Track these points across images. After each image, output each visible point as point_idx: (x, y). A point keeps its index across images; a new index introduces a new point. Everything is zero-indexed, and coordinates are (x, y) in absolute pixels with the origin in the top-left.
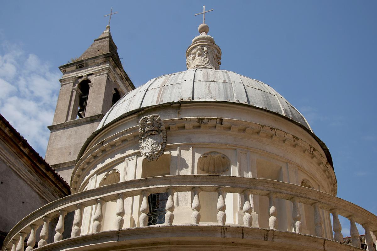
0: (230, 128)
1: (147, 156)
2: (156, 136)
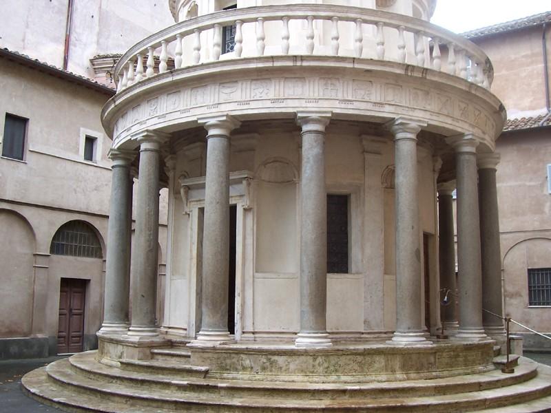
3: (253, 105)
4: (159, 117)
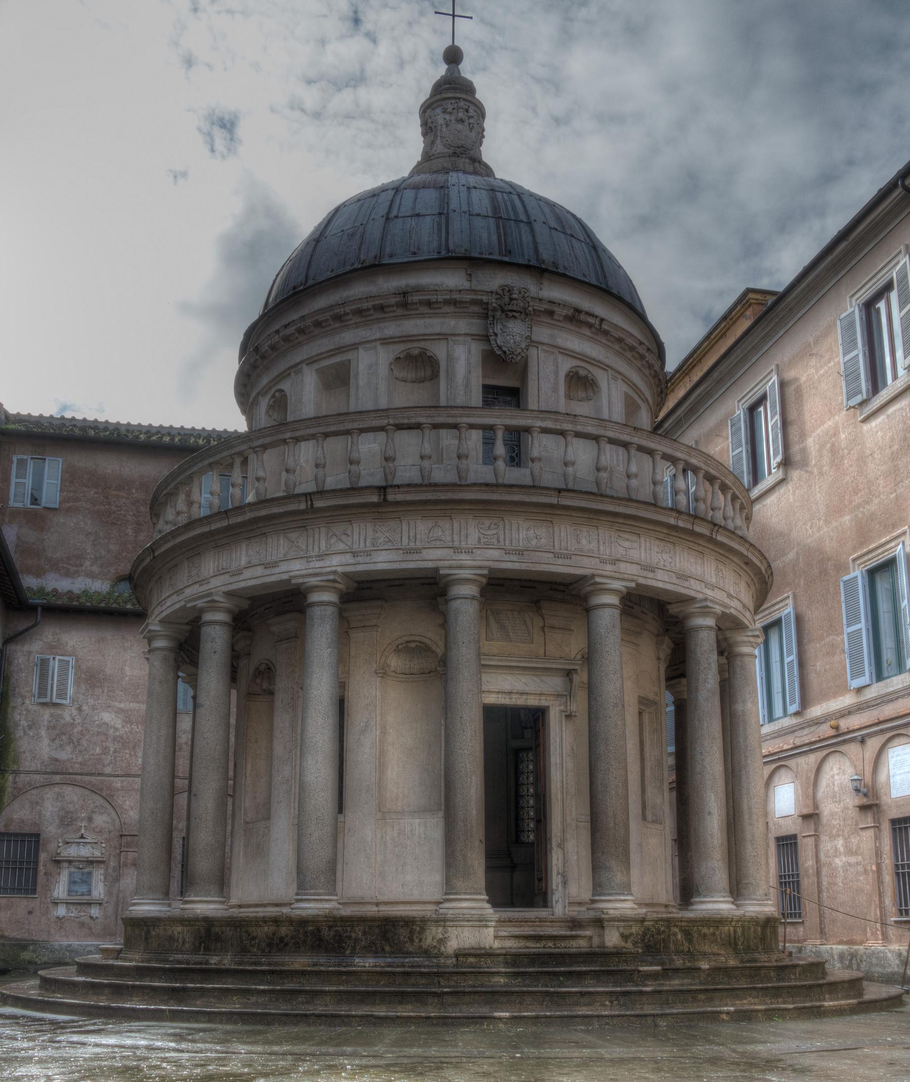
1: (505, 352)
3: (660, 575)
4: (507, 552)
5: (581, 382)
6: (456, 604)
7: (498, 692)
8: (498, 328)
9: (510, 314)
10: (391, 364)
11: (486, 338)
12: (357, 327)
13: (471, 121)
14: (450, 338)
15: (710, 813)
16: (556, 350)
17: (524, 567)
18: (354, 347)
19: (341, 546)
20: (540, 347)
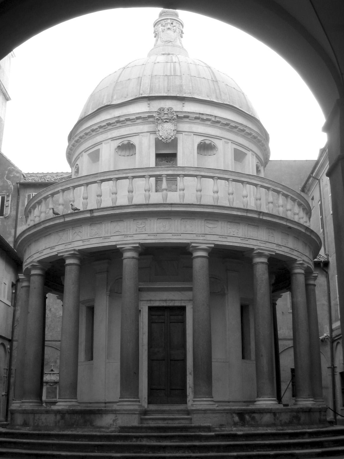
0: (218, 122)
1: (163, 138)
2: (169, 123)
3: (230, 239)
4: (149, 235)
5: (205, 148)
6: (125, 261)
7: (160, 300)
8: (160, 128)
9: (165, 120)
10: (116, 149)
11: (154, 132)
12: (102, 134)
13: (175, 28)
14: (140, 134)
15: (262, 356)
16: (192, 134)
17: (157, 241)
18: (100, 143)
19: (78, 238)
20: (184, 133)
